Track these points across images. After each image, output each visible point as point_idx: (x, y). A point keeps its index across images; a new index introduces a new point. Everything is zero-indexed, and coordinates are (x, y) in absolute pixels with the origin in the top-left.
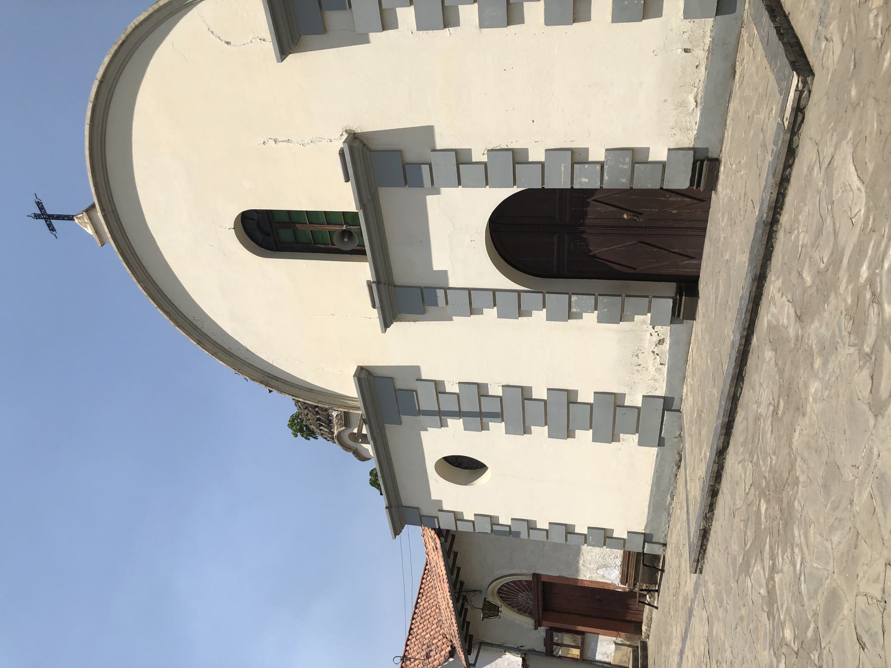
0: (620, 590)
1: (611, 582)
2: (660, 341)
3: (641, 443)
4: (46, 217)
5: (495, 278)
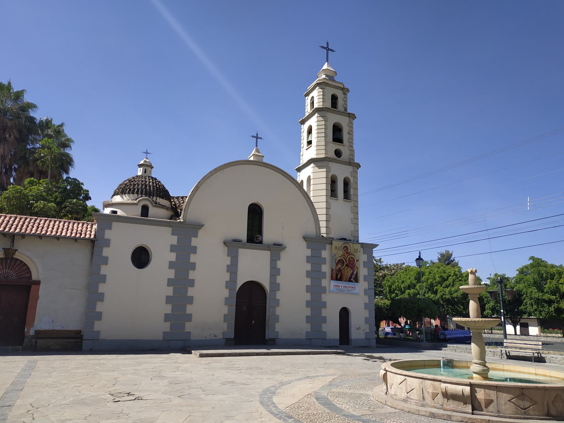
0: (26, 330)
1: (35, 325)
2: (216, 336)
3: (164, 333)
5: (240, 283)
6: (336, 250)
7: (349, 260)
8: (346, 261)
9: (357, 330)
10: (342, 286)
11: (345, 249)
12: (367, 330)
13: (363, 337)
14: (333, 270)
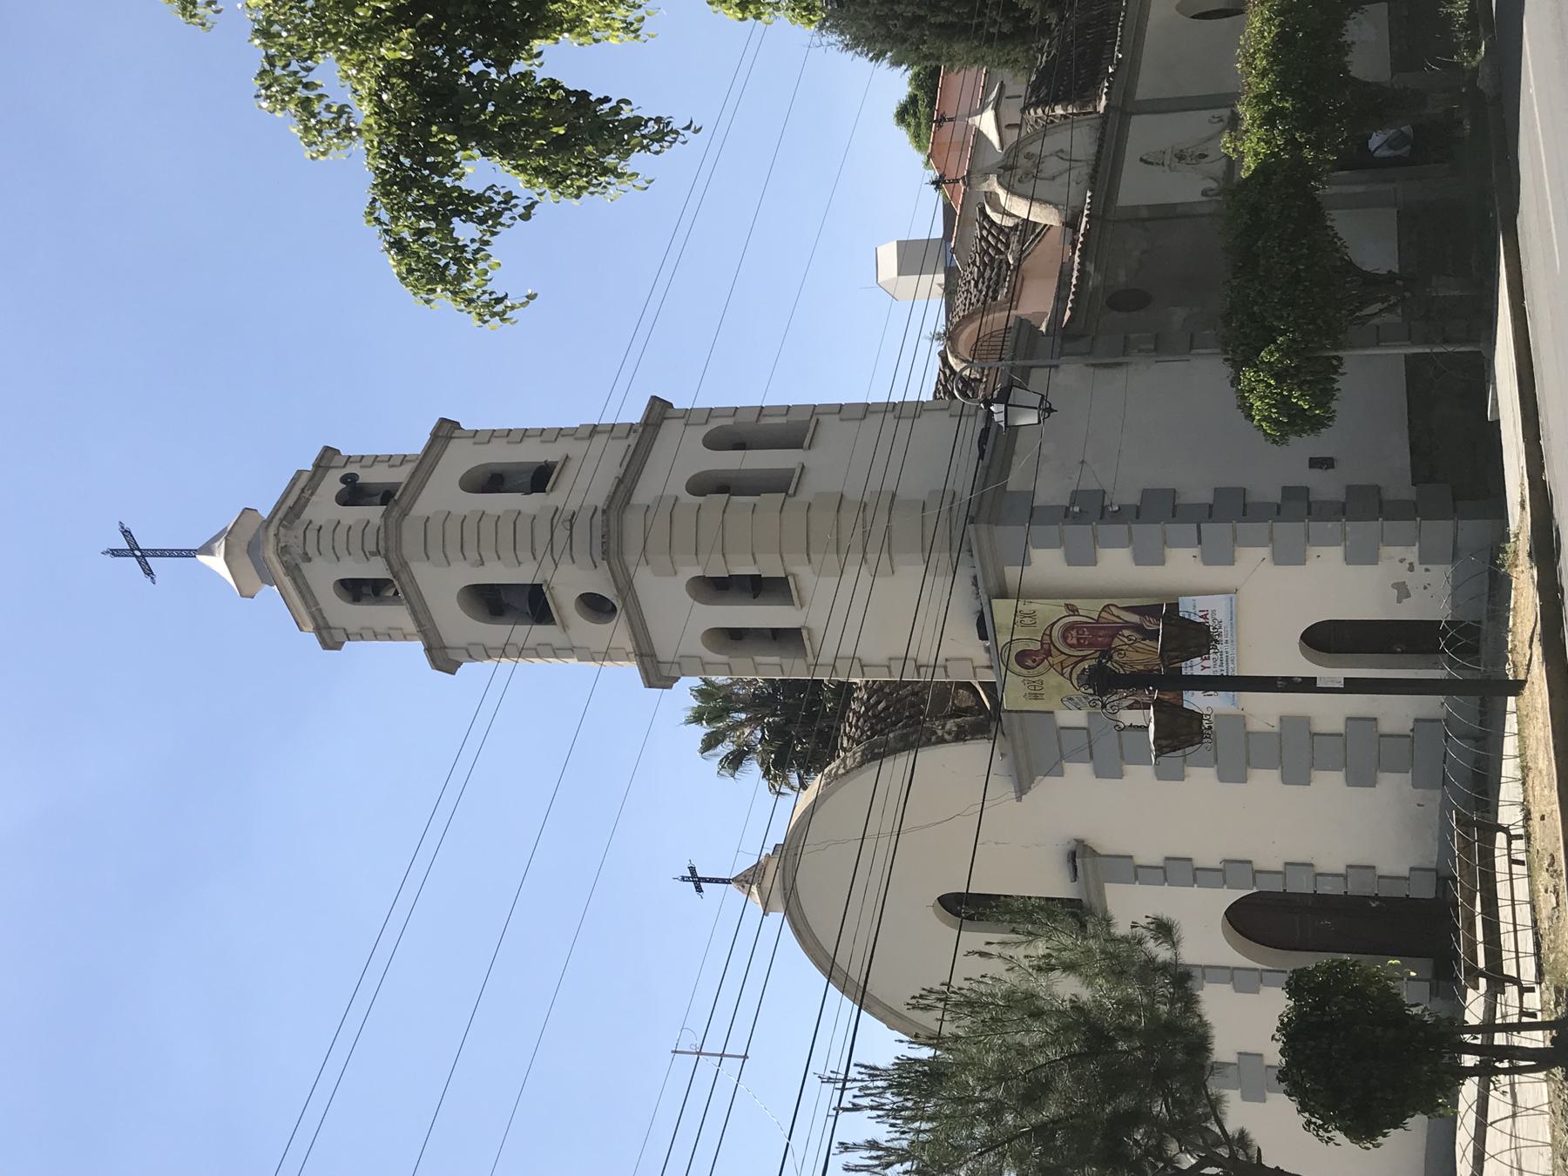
4: (697, 881)
6: (1044, 697)
7: (1079, 645)
8: (1084, 658)
9: (1408, 595)
10: (1205, 668)
11: (1029, 663)
12: (1412, 554)
13: (1440, 576)
14: (1137, 702)
